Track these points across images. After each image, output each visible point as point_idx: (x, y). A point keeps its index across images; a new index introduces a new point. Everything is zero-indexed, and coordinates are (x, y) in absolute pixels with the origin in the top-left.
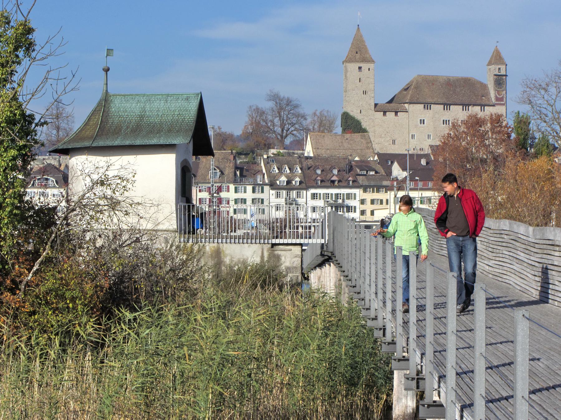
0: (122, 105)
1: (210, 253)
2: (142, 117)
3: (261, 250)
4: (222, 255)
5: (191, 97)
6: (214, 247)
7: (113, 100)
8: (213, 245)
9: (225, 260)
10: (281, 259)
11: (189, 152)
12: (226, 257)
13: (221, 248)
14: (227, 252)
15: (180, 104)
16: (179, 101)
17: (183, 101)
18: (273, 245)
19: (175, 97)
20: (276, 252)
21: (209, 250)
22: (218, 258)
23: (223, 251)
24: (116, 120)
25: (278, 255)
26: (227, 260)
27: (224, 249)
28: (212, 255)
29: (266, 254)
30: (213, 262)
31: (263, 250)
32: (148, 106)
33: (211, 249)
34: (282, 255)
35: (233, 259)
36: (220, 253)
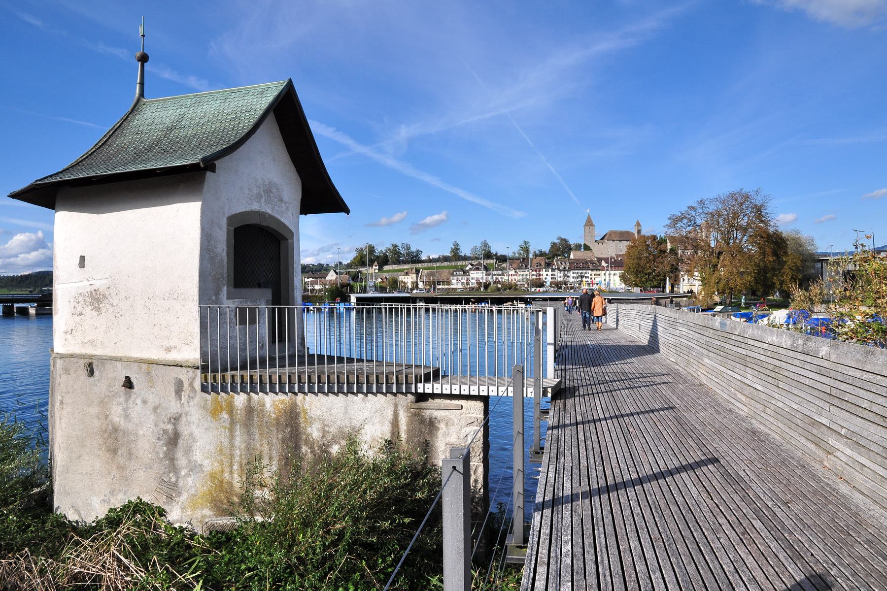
1: (273, 416)
2: (171, 129)
3: (392, 408)
4: (302, 420)
6: (284, 401)
7: (143, 110)
8: (282, 397)
10: (438, 429)
11: (281, 200)
12: (311, 424)
13: (299, 403)
14: (314, 413)
16: (247, 98)
18: (422, 397)
20: (426, 413)
21: (271, 409)
26: (314, 432)
27: (307, 406)
28: (277, 420)
31: (396, 406)
32: (191, 112)
36: (297, 415)
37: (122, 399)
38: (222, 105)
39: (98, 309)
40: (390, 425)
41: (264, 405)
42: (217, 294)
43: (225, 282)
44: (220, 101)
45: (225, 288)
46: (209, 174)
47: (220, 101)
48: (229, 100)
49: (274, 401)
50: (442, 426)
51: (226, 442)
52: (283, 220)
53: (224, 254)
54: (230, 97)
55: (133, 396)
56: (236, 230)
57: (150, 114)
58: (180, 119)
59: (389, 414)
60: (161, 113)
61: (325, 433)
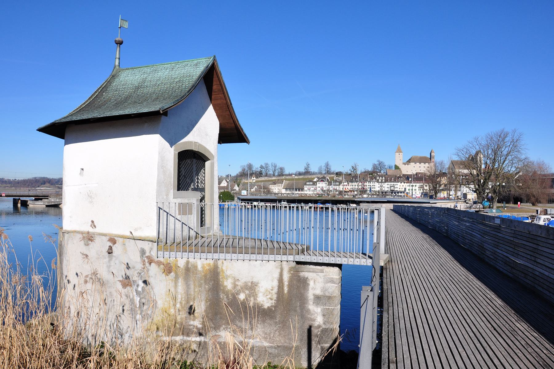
0: (126, 78)
2: (138, 88)
3: (279, 270)
5: (201, 62)
6: (209, 264)
9: (225, 284)
10: (309, 285)
12: (227, 279)
13: (220, 267)
15: (186, 70)
17: (190, 67)
19: (184, 64)
20: (302, 274)
22: (214, 281)
23: (222, 271)
24: (110, 94)
25: (304, 278)
26: (228, 284)
27: (224, 268)
28: (205, 276)
29: (286, 277)
30: (207, 287)
33: (203, 267)
34: (309, 278)
35: (237, 283)
37: (107, 260)
38: (170, 72)
39: (91, 202)
40: (277, 281)
41: (197, 267)
42: (167, 195)
43: (172, 187)
44: (169, 70)
45: (172, 191)
46: (163, 118)
47: (169, 70)
48: (175, 69)
49: (203, 265)
50: (311, 283)
51: (172, 290)
52: (207, 147)
53: (172, 169)
54: (176, 67)
55: (114, 259)
56: (179, 153)
57: (124, 78)
58: (144, 81)
59: (276, 275)
60: (131, 77)
61: (235, 286)
